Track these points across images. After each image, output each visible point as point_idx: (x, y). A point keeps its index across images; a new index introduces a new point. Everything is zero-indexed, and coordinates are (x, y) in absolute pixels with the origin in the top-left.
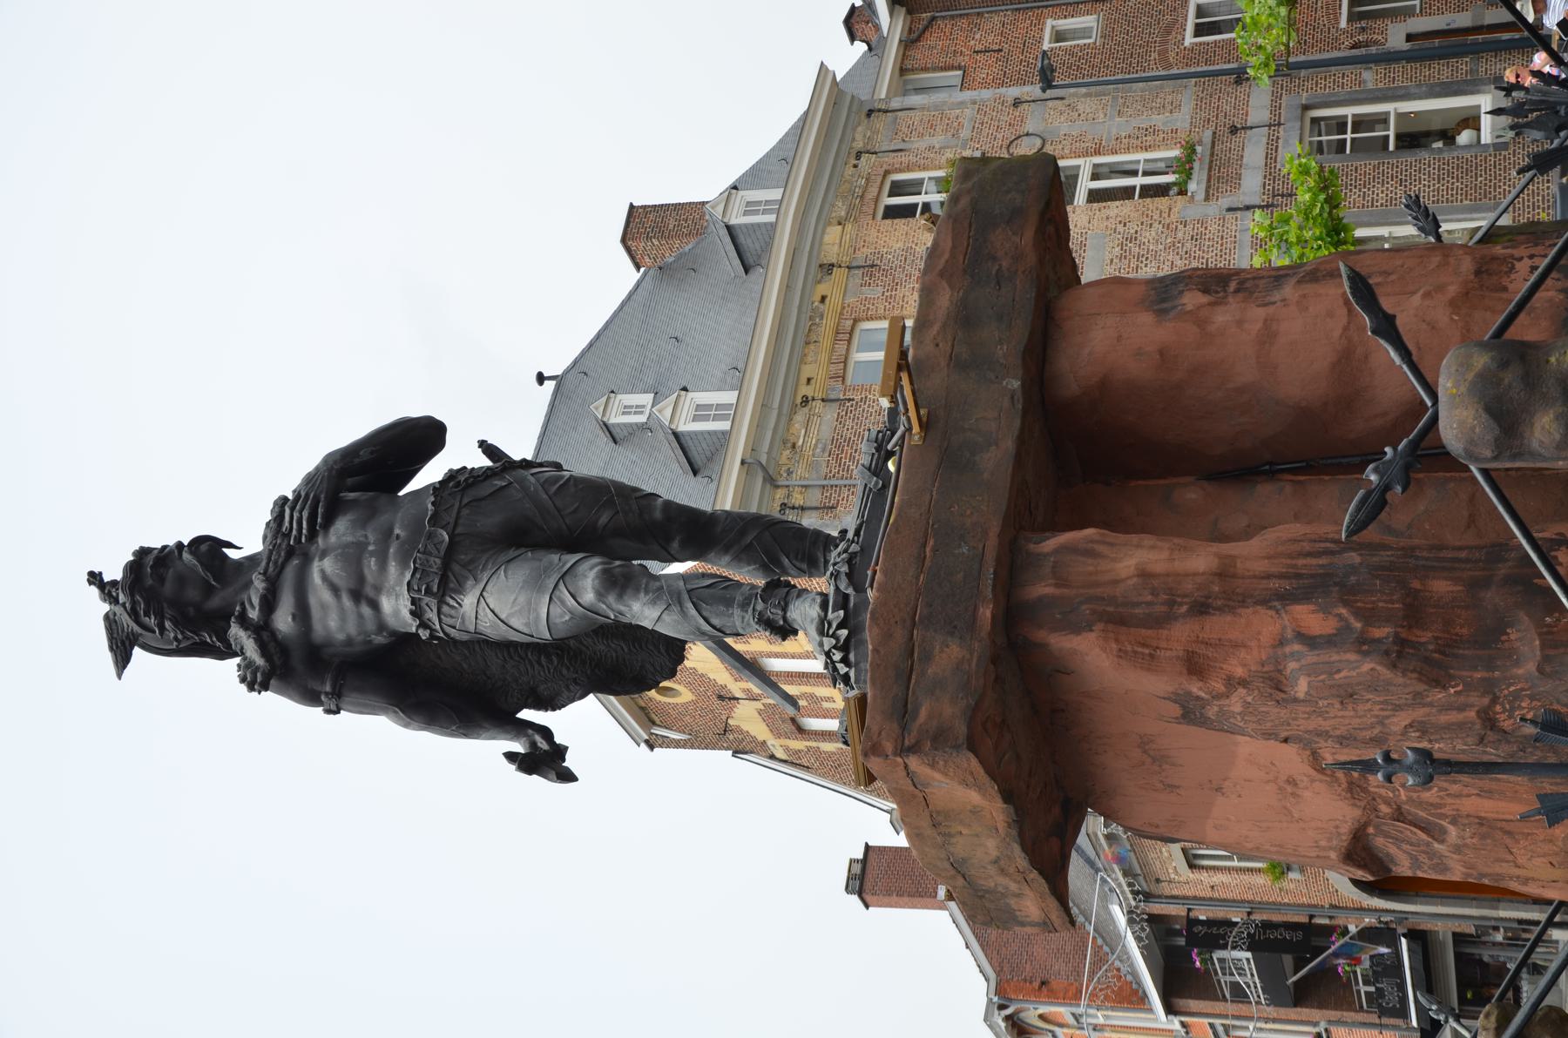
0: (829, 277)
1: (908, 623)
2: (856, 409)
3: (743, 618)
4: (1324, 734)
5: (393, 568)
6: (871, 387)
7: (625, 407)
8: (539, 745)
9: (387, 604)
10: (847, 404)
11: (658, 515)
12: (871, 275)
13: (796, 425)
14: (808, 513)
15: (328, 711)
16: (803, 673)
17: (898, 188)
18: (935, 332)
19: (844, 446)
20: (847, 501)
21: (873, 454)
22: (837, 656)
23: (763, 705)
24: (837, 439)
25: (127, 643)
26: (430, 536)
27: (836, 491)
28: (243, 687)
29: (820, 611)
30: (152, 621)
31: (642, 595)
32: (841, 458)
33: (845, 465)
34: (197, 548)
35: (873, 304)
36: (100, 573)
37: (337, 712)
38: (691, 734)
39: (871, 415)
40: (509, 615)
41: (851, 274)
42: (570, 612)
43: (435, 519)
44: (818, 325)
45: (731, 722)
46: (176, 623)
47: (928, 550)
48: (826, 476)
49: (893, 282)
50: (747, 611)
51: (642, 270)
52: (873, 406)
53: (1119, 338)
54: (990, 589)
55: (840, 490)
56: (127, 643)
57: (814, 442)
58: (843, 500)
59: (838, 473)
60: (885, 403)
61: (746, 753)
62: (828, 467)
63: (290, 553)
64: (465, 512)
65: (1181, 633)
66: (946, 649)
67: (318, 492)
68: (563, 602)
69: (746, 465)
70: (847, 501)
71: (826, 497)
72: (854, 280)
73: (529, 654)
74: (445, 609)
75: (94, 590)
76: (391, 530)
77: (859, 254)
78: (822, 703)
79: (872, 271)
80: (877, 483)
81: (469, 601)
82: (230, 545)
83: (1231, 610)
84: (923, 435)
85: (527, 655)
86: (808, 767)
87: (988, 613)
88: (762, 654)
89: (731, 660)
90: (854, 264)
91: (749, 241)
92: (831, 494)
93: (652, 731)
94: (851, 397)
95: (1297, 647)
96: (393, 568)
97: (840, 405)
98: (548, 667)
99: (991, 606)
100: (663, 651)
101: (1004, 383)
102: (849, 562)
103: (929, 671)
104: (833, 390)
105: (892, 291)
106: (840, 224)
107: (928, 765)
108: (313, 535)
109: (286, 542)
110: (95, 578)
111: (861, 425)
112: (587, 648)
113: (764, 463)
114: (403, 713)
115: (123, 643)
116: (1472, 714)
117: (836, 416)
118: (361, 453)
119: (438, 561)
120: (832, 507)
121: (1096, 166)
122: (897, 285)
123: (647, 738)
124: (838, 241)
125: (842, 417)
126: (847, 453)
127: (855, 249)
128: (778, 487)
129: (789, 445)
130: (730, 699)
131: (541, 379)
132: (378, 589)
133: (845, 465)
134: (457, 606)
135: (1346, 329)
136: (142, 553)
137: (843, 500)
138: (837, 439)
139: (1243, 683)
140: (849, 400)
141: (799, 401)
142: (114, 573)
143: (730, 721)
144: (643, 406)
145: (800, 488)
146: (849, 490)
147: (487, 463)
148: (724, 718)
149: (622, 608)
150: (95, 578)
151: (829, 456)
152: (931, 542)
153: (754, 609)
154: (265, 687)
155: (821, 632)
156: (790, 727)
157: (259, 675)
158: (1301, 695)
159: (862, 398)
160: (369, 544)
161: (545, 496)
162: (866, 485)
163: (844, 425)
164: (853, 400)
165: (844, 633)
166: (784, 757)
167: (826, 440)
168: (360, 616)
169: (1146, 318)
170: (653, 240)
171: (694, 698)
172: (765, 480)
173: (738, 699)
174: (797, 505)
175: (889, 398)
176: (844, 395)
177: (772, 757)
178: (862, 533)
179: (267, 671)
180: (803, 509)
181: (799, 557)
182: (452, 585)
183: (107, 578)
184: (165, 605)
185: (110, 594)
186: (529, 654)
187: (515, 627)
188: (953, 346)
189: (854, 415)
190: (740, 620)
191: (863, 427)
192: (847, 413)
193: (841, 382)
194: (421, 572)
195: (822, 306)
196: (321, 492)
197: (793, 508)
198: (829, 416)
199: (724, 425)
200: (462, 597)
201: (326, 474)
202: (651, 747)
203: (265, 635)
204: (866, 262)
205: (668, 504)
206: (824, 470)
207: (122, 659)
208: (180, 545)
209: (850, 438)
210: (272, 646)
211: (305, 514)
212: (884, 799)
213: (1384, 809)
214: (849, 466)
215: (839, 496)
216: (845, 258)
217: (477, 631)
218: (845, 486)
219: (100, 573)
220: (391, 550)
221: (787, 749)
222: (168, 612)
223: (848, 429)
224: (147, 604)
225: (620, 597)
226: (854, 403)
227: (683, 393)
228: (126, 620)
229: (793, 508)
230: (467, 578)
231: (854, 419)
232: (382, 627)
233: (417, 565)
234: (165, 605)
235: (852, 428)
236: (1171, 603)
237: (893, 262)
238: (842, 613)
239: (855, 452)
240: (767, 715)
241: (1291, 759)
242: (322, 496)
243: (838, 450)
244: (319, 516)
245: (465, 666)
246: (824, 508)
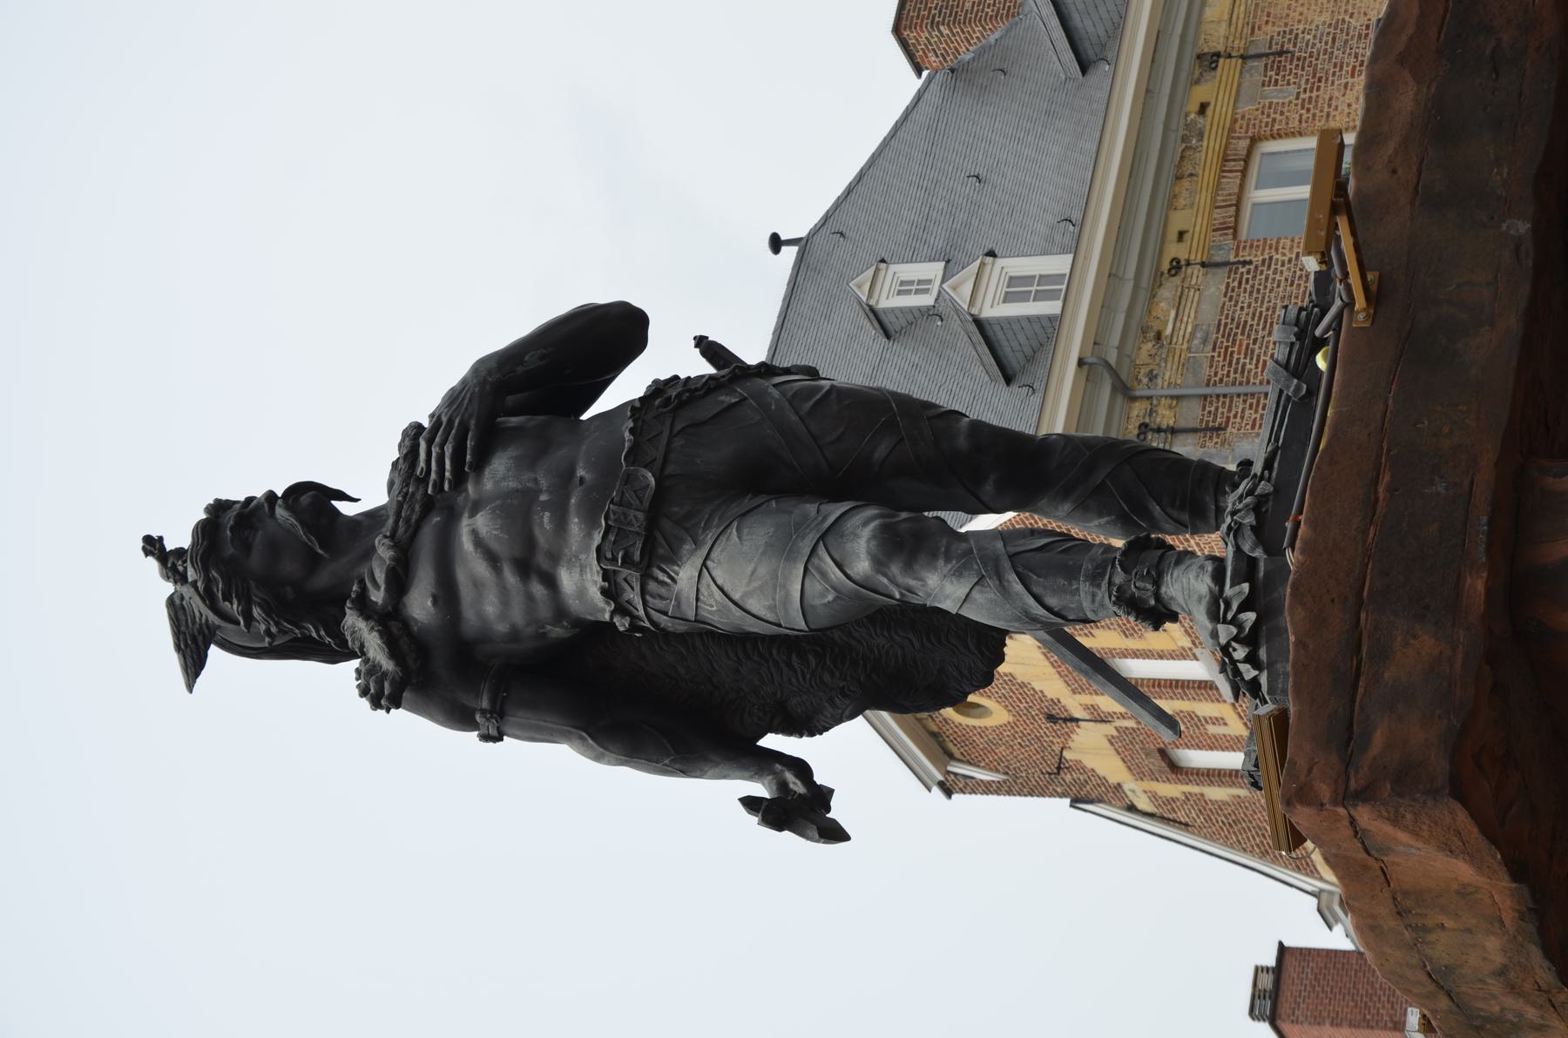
0: (1213, 73)
2: (1255, 277)
3: (1094, 595)
5: (575, 526)
6: (1278, 242)
7: (902, 283)
8: (791, 786)
9: (568, 580)
10: (1241, 270)
11: (962, 442)
12: (1278, 68)
13: (1162, 304)
14: (1181, 438)
15: (486, 738)
16: (1177, 681)
18: (1390, 152)
19: (1236, 334)
20: (1242, 418)
21: (1292, 344)
22: (1240, 653)
23: (1116, 728)
24: (1226, 324)
25: (200, 639)
26: (629, 479)
27: (1224, 403)
28: (365, 703)
29: (1212, 585)
30: (235, 607)
31: (941, 562)
32: (1232, 353)
33: (1238, 363)
34: (296, 500)
35: (1282, 113)
36: (161, 539)
37: (499, 739)
38: (1007, 773)
39: (1279, 286)
40: (746, 594)
41: (1247, 67)
42: (834, 588)
43: (634, 454)
44: (1195, 149)
45: (1067, 755)
46: (268, 611)
47: (1381, 489)
48: (1209, 380)
49: (1314, 77)
50: (1099, 586)
51: (925, 74)
52: (1282, 272)
54: (1482, 548)
55: (1231, 401)
56: (200, 639)
57: (1189, 329)
58: (1235, 416)
59: (1228, 376)
60: (1312, 264)
61: (1091, 802)
62: (1211, 367)
63: (428, 506)
64: (678, 443)
66: (1412, 641)
67: (466, 415)
68: (824, 575)
69: (1086, 368)
70: (1242, 418)
71: (1210, 412)
72: (1251, 76)
73: (774, 652)
74: (652, 586)
75: (152, 564)
76: (571, 471)
77: (1260, 36)
78: (1208, 727)
79: (1280, 62)
80: (1298, 388)
81: (686, 574)
82: (342, 496)
84: (1372, 311)
85: (771, 654)
86: (1186, 825)
87: (1480, 586)
88: (1114, 653)
89: (1076, 659)
90: (1252, 52)
91: (1088, 23)
92: (1217, 409)
93: (950, 768)
94: (1248, 259)
96: (575, 526)
97: (1230, 271)
98: (803, 672)
99: (1485, 575)
100: (972, 647)
101: (1504, 226)
102: (1257, 509)
103: (1386, 675)
104: (1220, 248)
105: (1311, 91)
107: (1388, 819)
108: (459, 480)
109: (421, 492)
110: (153, 546)
111: (1262, 303)
112: (859, 641)
113: (1112, 361)
114: (592, 738)
115: (194, 639)
117: (1223, 288)
118: (526, 358)
119: (641, 515)
122: (1320, 81)
123: (941, 778)
124: (1226, 17)
125: (1233, 291)
126: (1240, 345)
127: (1253, 28)
128: (1134, 399)
129: (1152, 335)
130: (1065, 720)
131: (776, 243)
132: (555, 558)
133: (1238, 363)
134: (668, 581)
136: (219, 509)
137: (1235, 416)
138: (1226, 324)
140: (1245, 263)
141: (1166, 266)
142: (179, 537)
143: (1065, 754)
144: (929, 282)
145: (1169, 401)
146: (1245, 401)
147: (709, 369)
148: (1057, 748)
149: (912, 583)
150: (153, 546)
151: (1214, 350)
152: (1386, 479)
153: (1110, 583)
154: (395, 702)
155: (1215, 616)
156: (1157, 763)
157: (387, 685)
159: (1264, 260)
160: (540, 491)
161: (794, 418)
162: (1281, 392)
163: (1237, 302)
164: (1250, 262)
165: (1250, 617)
166: (1150, 808)
167: (1209, 325)
168: (530, 598)
170: (942, 28)
171: (1011, 719)
172: (1114, 389)
173: (1077, 720)
174: (1164, 426)
175: (1319, 256)
176: (1237, 255)
177: (1132, 808)
178: (1276, 465)
179: (398, 679)
180: (1173, 431)
181: (1178, 503)
182: (661, 551)
183: (170, 545)
184: (253, 584)
185: (174, 569)
186: (774, 652)
187: (754, 611)
188: (1420, 172)
189: (1253, 287)
190: (1089, 598)
191: (1265, 305)
192: (1240, 283)
193: (1231, 237)
194: (616, 532)
195: (1201, 120)
196: (470, 417)
197: (1159, 430)
198: (1213, 290)
199: (1052, 307)
200: (676, 568)
201: (477, 390)
202: (948, 793)
203: (395, 626)
204: (1270, 47)
205: (978, 427)
206: (1206, 371)
207: (193, 664)
208: (271, 496)
209: (1246, 322)
211: (448, 449)
212: (1307, 875)
214: (1244, 365)
215: (1230, 410)
216: (1237, 42)
217: (698, 618)
218: (1239, 396)
219: (161, 539)
220: (573, 501)
221: (1154, 797)
223: (1242, 308)
224: (228, 583)
225: (908, 566)
226: (1252, 267)
227: (989, 260)
228: (198, 606)
229: (1159, 430)
230: (682, 541)
231: (1251, 292)
232: (560, 612)
233: (610, 523)
234: (253, 584)
235: (1249, 306)
237: (1314, 44)
238: (1246, 587)
239: (1254, 343)
240: (1123, 744)
242: (473, 422)
243: (1228, 341)
244: (469, 452)
245: (681, 670)
246: (1207, 429)
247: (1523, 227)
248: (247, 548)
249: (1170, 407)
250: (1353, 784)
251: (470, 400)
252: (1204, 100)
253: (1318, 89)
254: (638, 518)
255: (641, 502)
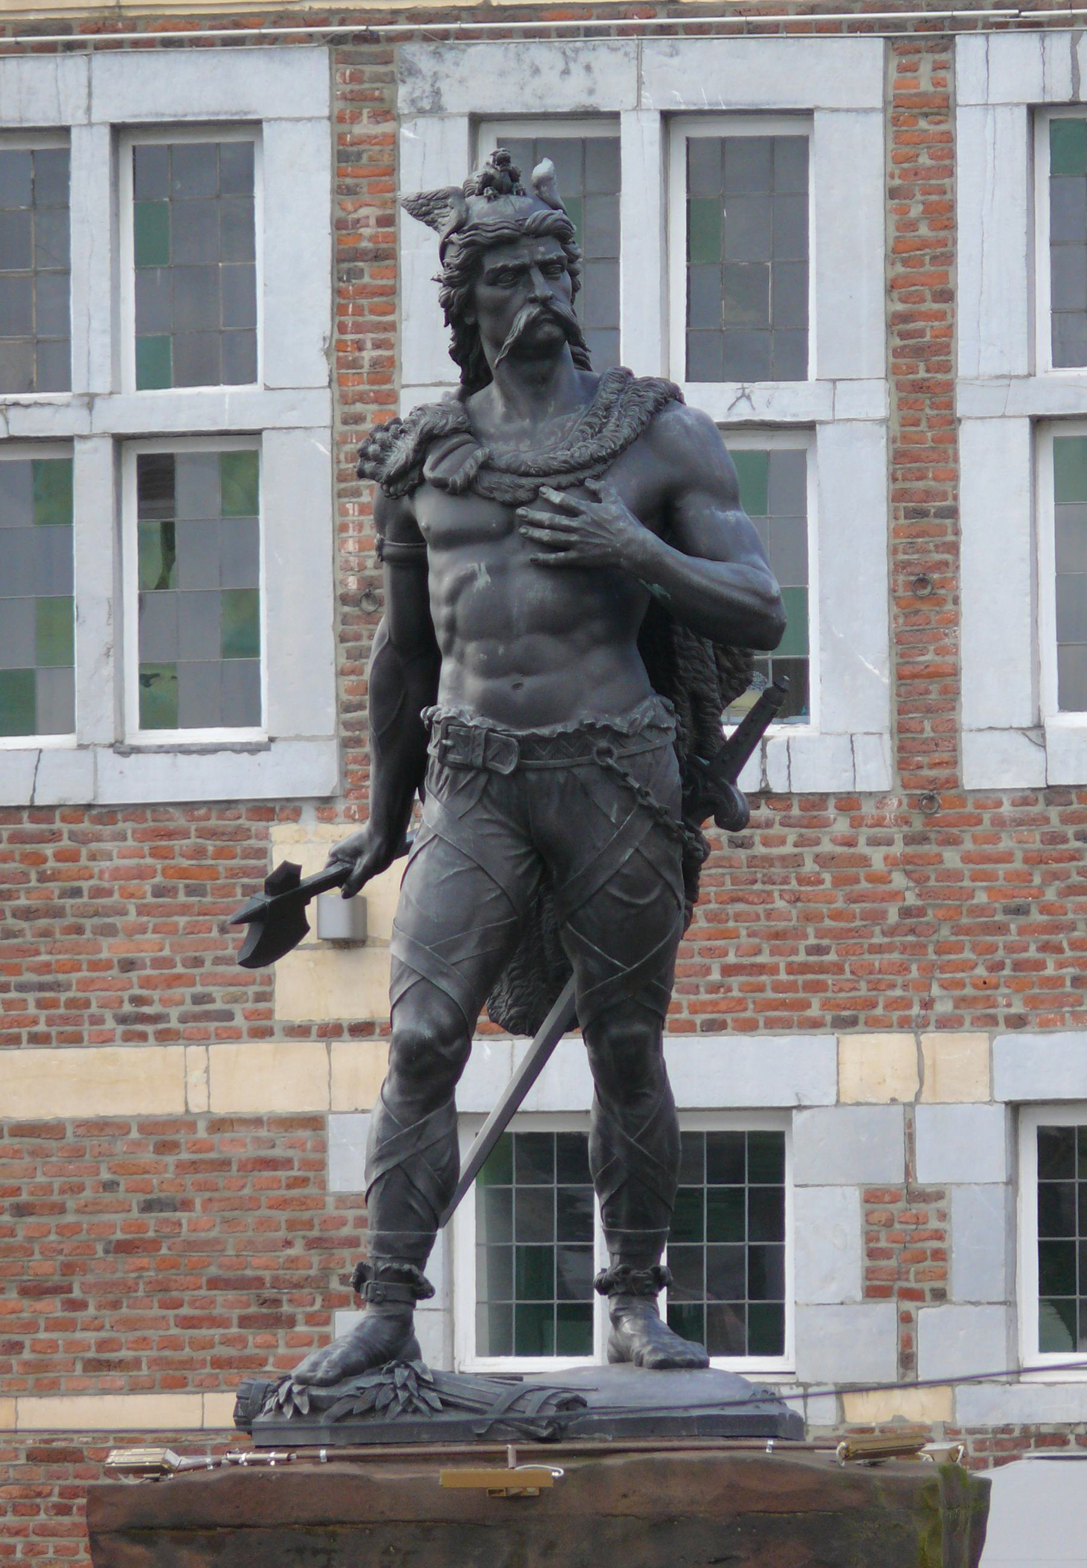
1: (238, 1521)
165: (288, 1412)
184: (463, 290)
196: (581, 550)
242: (572, 554)
248: (493, 283)
250: (101, 1538)
251: (597, 545)
255: (493, 759)
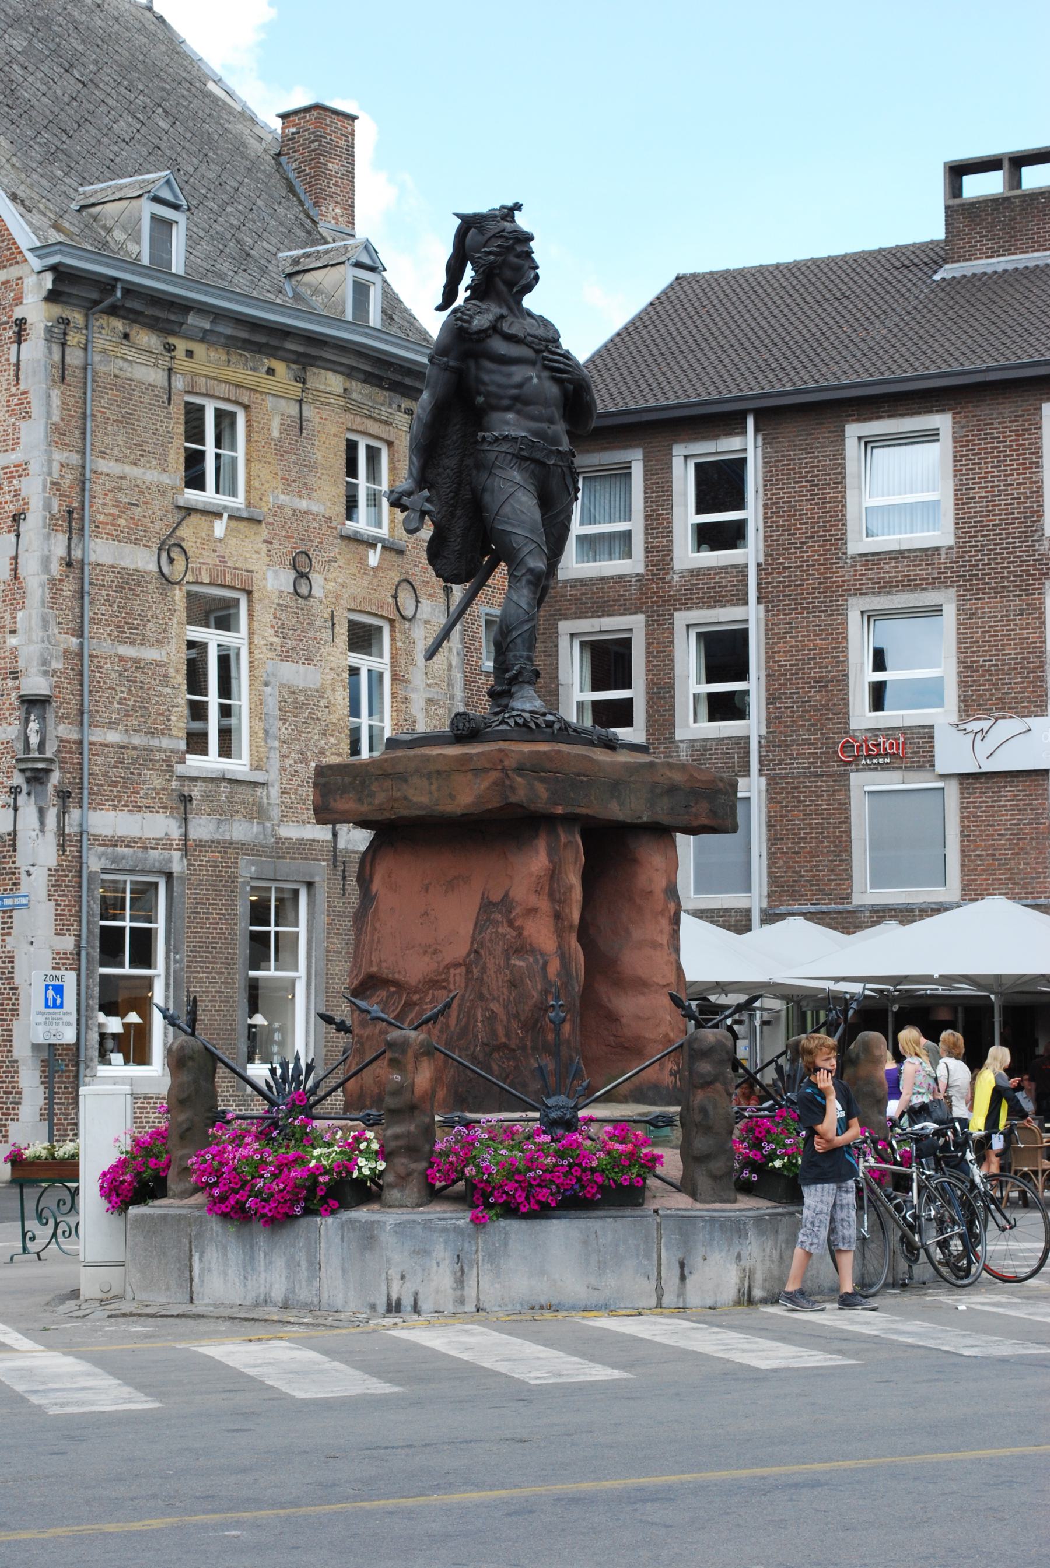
4: (484, 970)
9: (510, 416)
17: (373, 455)
22: (520, 721)
35: (263, 428)
44: (245, 364)
53: (657, 870)
57: (130, 358)
65: (544, 905)
75: (510, 204)
81: (516, 476)
83: (556, 931)
87: (560, 812)
95: (541, 962)
106: (345, 390)
108: (546, 368)
110: (518, 207)
116: (503, 1040)
120: (63, 378)
121: (381, 675)
132: (518, 412)
135: (658, 984)
139: (520, 935)
145: (84, 342)
150: (518, 207)
157: (465, 325)
158: (513, 962)
164: (169, 404)
169: (664, 884)
170: (316, 143)
174: (68, 338)
185: (507, 215)
195: (265, 369)
197: (65, 334)
210: (483, 335)
211: (562, 366)
213: (416, 997)
222: (500, 259)
236: (560, 902)
241: (459, 950)
245: (449, 442)
247: (645, 819)
249: (79, 343)
252: (277, 371)
253: (276, 454)
254: (539, 456)
